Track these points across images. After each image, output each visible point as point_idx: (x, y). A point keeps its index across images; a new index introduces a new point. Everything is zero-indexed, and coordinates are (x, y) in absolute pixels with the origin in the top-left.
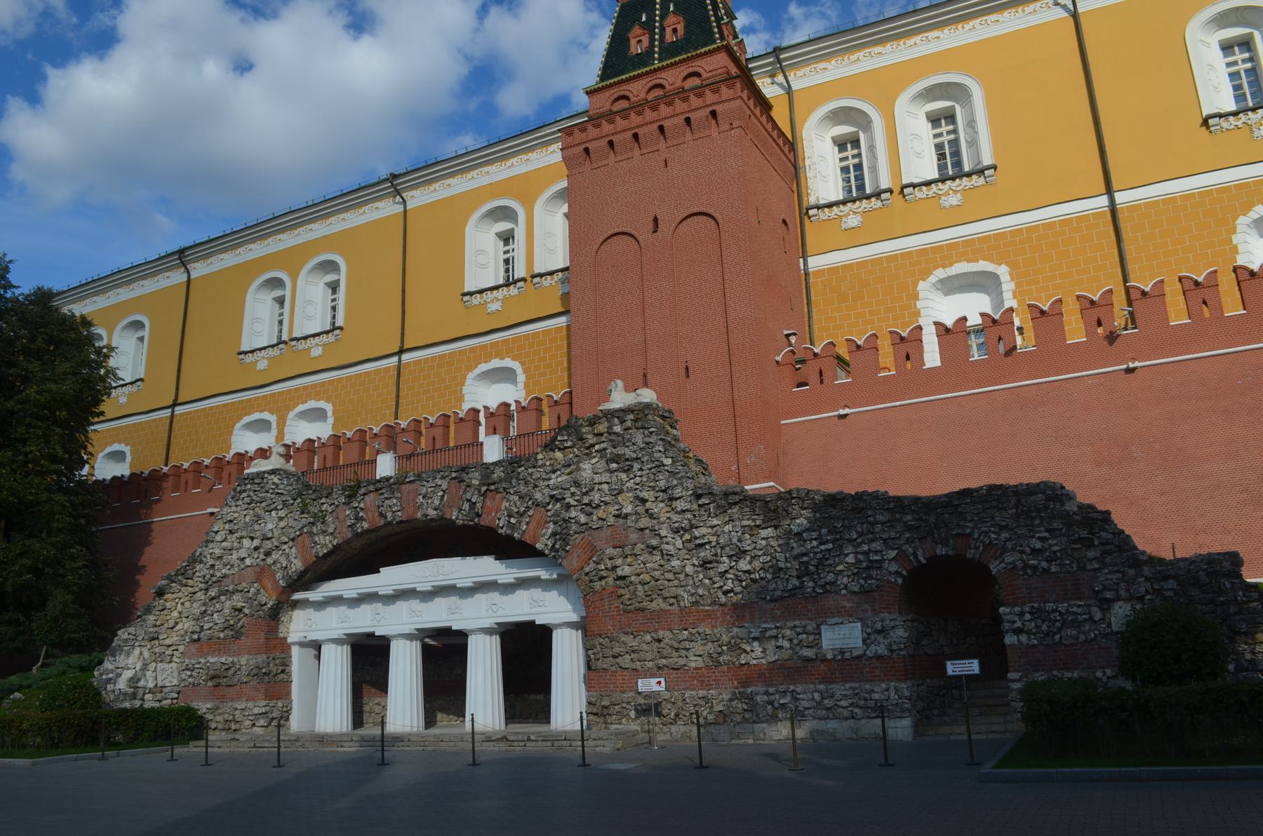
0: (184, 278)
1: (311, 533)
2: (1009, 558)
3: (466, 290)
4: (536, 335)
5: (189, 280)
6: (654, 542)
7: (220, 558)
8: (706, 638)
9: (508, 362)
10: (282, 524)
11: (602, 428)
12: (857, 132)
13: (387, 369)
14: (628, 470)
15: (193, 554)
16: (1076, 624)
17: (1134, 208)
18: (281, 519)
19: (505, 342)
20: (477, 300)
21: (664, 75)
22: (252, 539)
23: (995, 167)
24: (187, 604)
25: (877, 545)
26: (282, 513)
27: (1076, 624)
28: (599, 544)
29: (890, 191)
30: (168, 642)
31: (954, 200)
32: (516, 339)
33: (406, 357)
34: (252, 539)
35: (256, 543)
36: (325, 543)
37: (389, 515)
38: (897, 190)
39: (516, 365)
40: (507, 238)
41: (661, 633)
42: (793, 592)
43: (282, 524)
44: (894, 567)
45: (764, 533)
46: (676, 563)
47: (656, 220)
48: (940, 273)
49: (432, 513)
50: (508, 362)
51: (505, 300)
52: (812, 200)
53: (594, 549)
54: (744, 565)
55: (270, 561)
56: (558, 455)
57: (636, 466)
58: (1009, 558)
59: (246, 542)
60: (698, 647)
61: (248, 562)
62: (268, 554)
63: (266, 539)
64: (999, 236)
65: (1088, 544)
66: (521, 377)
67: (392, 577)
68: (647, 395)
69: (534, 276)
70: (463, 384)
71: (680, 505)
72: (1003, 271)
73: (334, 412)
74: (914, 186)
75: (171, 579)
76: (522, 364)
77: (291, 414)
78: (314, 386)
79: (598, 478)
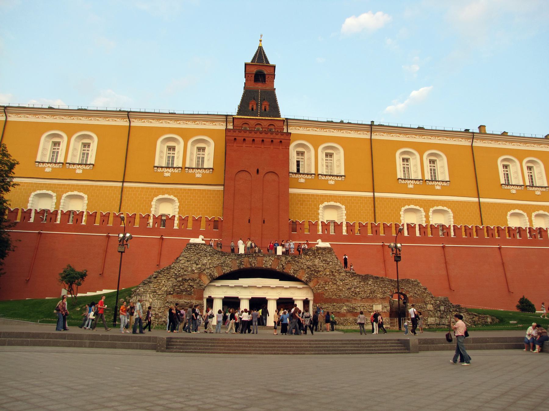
0: (4, 119)
1: (222, 266)
2: (411, 294)
3: (156, 165)
4: (185, 190)
5: (6, 121)
6: (335, 282)
7: (183, 269)
8: (347, 306)
9: (172, 197)
10: (210, 261)
11: (320, 251)
12: (304, 152)
13: (116, 187)
14: (328, 264)
15: (170, 266)
16: (422, 308)
17: (379, 198)
18: (209, 260)
19: (171, 189)
20: (160, 170)
21: (262, 121)
22: (197, 264)
23: (344, 176)
24: (166, 282)
25: (386, 289)
26: (209, 258)
27: (422, 308)
28: (319, 281)
29: (315, 174)
30: (159, 293)
31: (332, 182)
32: (176, 189)
33: (126, 184)
34: (197, 264)
35: (200, 266)
36: (227, 270)
37: (253, 265)
38: (316, 175)
39: (176, 199)
40: (171, 148)
41: (335, 304)
42: (368, 297)
43: (210, 261)
44: (389, 294)
45: (362, 283)
46: (341, 288)
47: (258, 171)
48: (326, 204)
49: (269, 267)
50: (172, 197)
51: (172, 173)
52: (290, 171)
53: (318, 282)
54: (358, 290)
55: (205, 272)
56: (308, 257)
57: (331, 263)
58: (411, 294)
59: (195, 265)
60: (345, 308)
61: (196, 271)
62: (204, 270)
63: (204, 265)
64: (344, 197)
65: (424, 293)
66: (178, 204)
67: (243, 281)
68: (327, 245)
69: (186, 168)
70: (152, 201)
71: (342, 274)
72: (343, 207)
73: (88, 199)
74: (322, 175)
75: (159, 273)
76: (178, 199)
77: (65, 195)
78: (78, 185)
79: (320, 265)
